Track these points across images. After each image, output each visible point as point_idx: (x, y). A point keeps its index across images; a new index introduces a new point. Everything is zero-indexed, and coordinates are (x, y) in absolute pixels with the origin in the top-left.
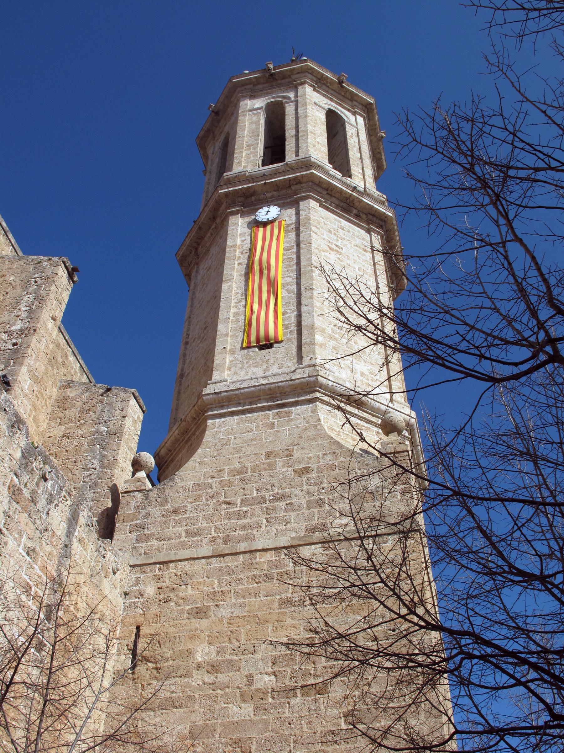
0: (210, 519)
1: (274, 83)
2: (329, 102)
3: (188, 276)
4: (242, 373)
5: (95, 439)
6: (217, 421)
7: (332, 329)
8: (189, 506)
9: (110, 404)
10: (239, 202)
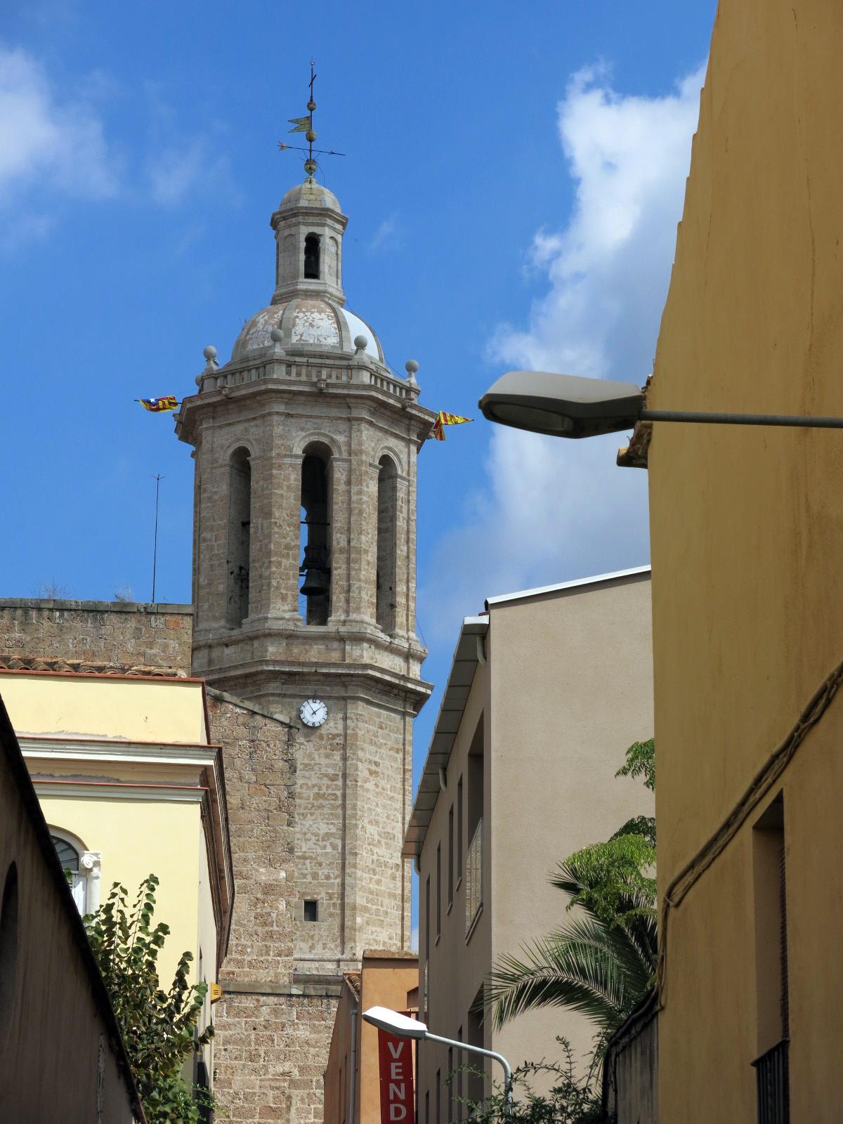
1: (320, 400)
10: (281, 679)
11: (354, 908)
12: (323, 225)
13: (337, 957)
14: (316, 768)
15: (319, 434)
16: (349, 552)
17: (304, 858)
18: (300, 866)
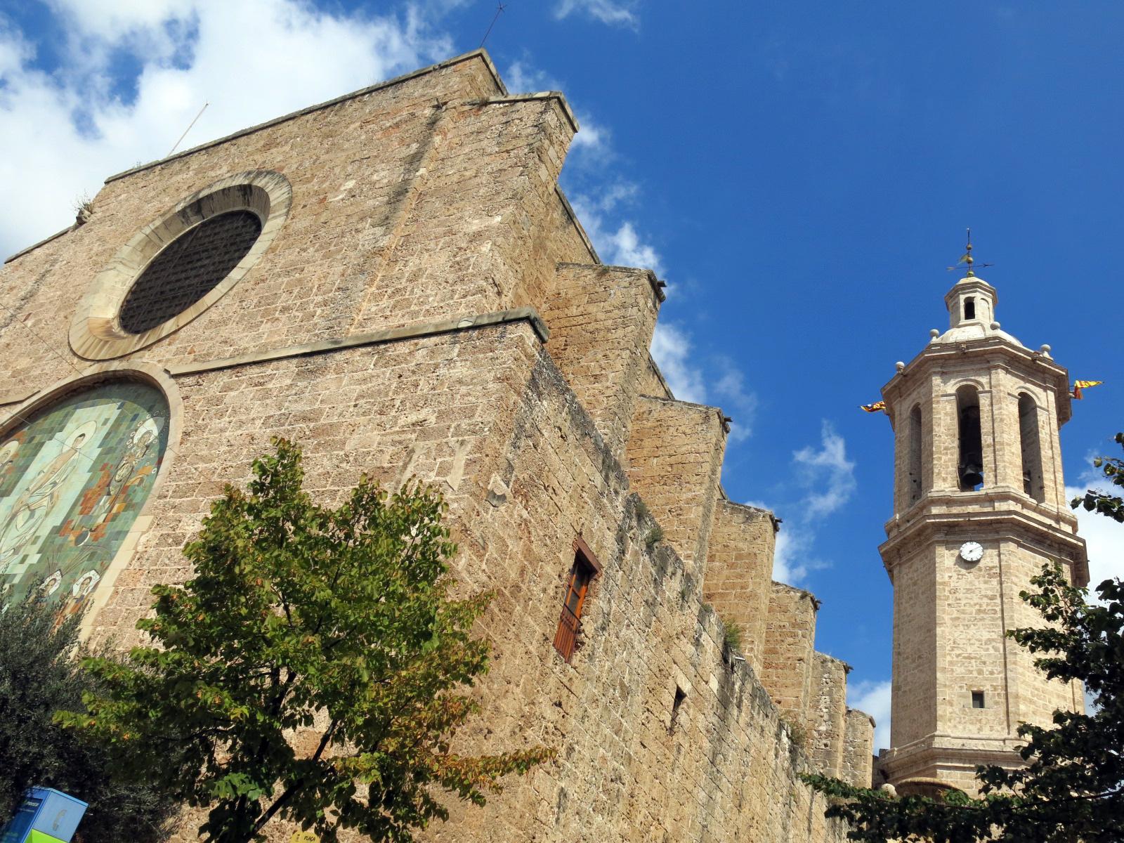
1: (966, 360)
2: (1022, 383)
3: (890, 571)
4: (961, 727)
6: (945, 772)
7: (1032, 693)
9: (853, 726)
11: (1017, 696)
12: (975, 292)
13: (1003, 738)
14: (977, 591)
15: (966, 380)
16: (994, 446)
17: (969, 658)
18: (966, 664)
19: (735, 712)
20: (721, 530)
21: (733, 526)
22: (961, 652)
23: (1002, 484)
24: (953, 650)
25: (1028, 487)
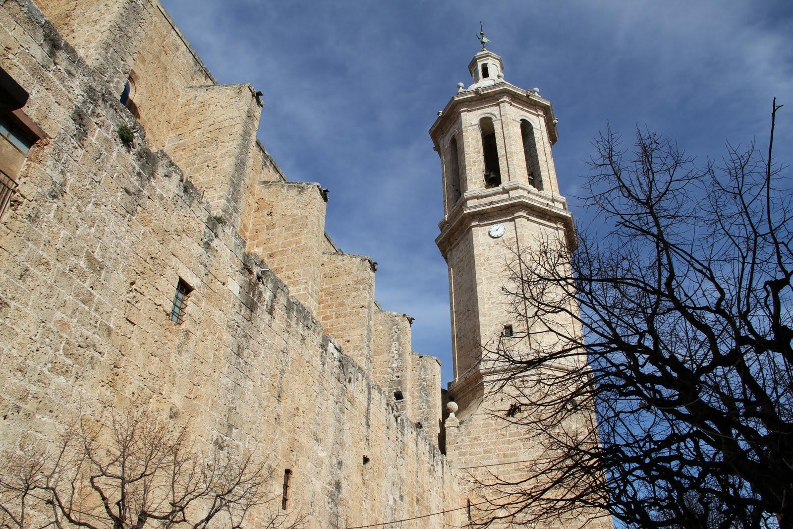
0: (494, 443)
3: (446, 258)
5: (421, 389)
8: (483, 436)
9: (424, 367)
12: (488, 59)
19: (267, 317)
20: (280, 204)
21: (290, 199)
22: (495, 300)
23: (513, 180)
24: (489, 300)
25: (531, 182)
